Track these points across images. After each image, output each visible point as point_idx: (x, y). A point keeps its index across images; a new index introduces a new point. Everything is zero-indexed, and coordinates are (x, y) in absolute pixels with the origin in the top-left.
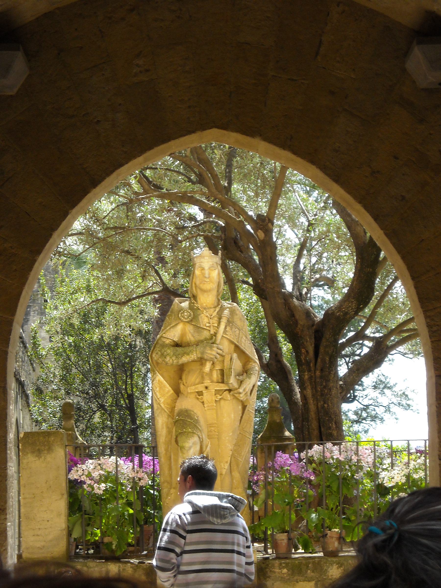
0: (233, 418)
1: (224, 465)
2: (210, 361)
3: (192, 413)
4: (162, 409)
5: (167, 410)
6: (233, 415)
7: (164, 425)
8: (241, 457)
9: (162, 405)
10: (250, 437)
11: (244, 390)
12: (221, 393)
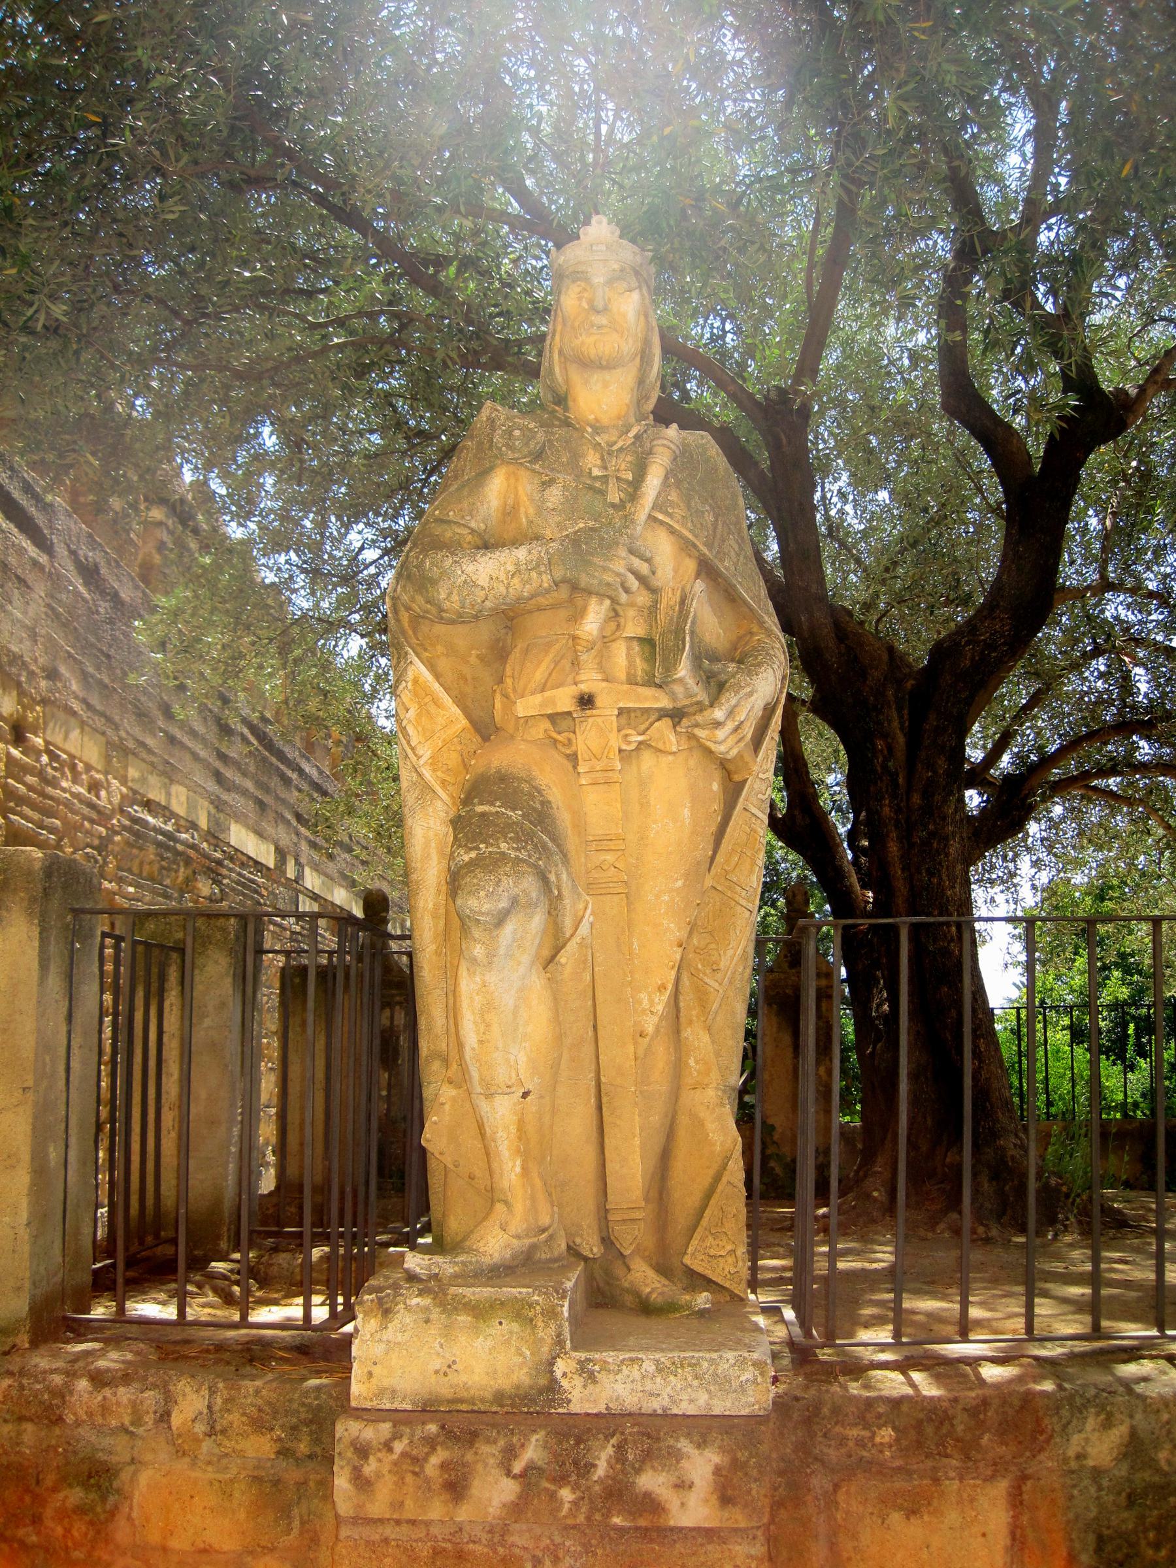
0: (687, 821)
1: (651, 1002)
2: (601, 596)
3: (525, 787)
6: (686, 812)
8: (719, 976)
9: (427, 774)
10: (750, 906)
11: (731, 714)
12: (643, 727)
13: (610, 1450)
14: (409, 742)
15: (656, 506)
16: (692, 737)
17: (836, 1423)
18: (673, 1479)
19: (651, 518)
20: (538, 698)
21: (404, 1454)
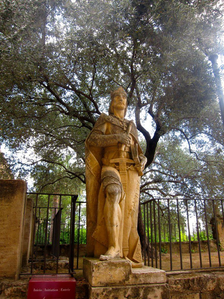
4: (92, 174)
5: (95, 174)
7: (92, 184)
9: (92, 172)
13: (143, 291)
14: (89, 166)
15: (131, 132)
17: (171, 284)
18: (154, 296)
19: (130, 133)
20: (113, 160)
21: (106, 295)
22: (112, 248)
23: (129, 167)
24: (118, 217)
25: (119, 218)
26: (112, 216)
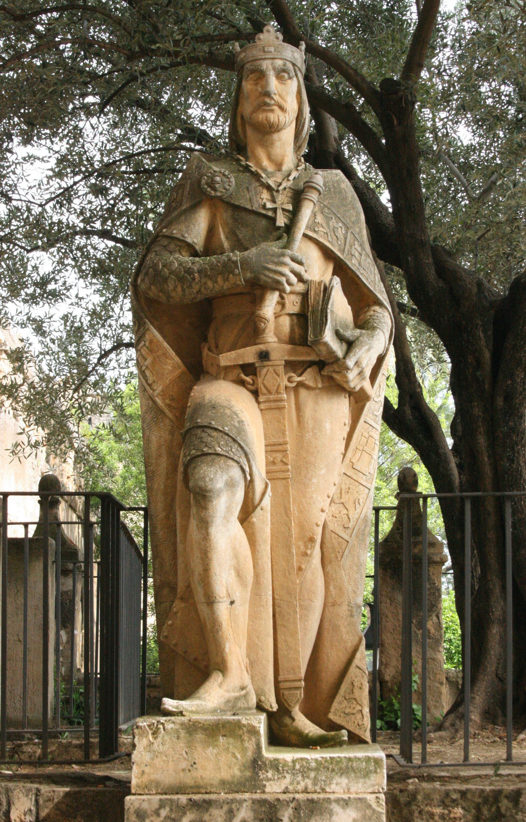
3: (228, 412)
4: (159, 411)
5: (171, 411)
7: (164, 447)
8: (349, 531)
9: (159, 401)
10: (369, 486)
11: (357, 363)
12: (299, 372)
13: (290, 811)
16: (331, 378)
17: (427, 805)
20: (233, 354)
22: (216, 678)
23: (299, 379)
24: (233, 572)
25: (239, 574)
26: (206, 570)
